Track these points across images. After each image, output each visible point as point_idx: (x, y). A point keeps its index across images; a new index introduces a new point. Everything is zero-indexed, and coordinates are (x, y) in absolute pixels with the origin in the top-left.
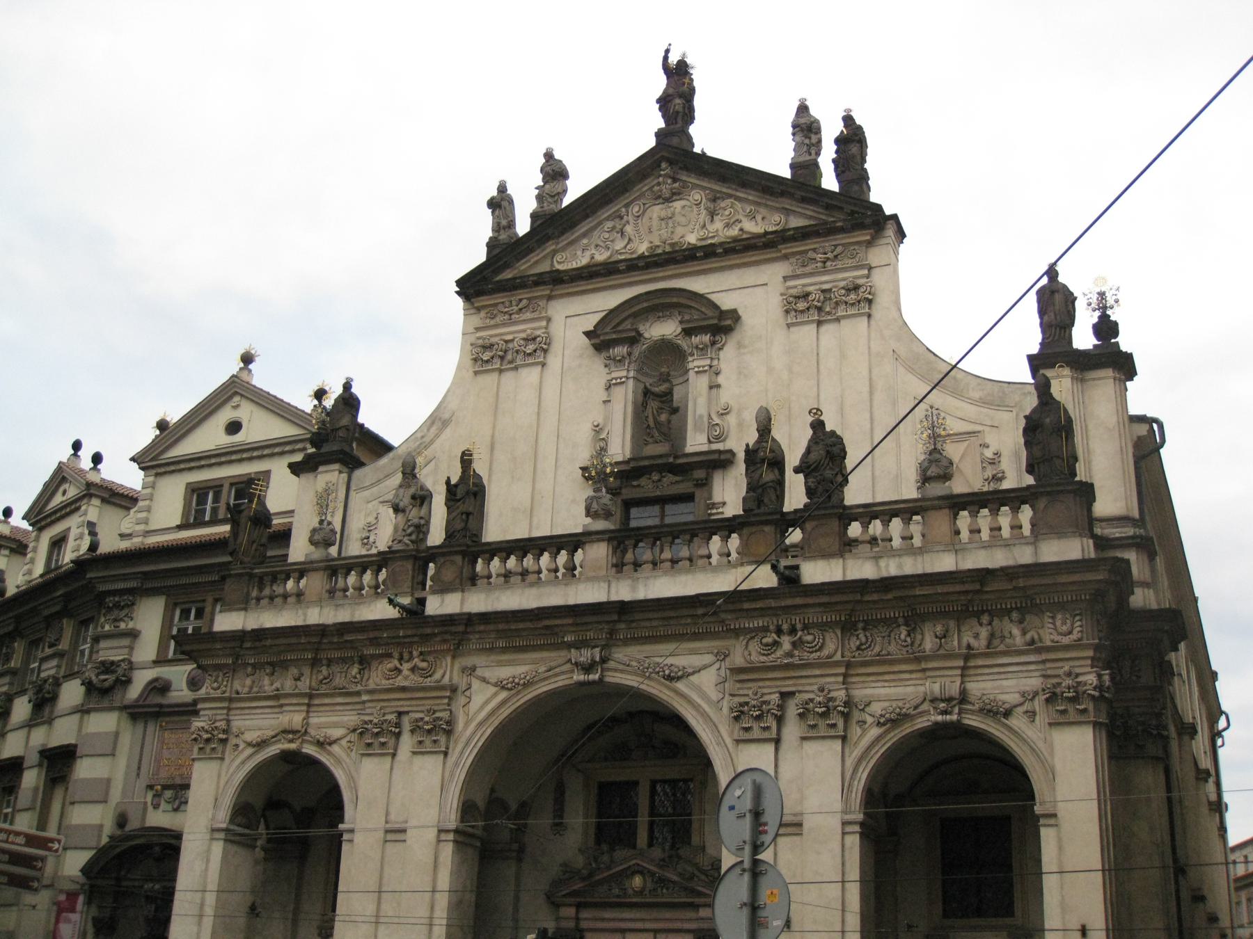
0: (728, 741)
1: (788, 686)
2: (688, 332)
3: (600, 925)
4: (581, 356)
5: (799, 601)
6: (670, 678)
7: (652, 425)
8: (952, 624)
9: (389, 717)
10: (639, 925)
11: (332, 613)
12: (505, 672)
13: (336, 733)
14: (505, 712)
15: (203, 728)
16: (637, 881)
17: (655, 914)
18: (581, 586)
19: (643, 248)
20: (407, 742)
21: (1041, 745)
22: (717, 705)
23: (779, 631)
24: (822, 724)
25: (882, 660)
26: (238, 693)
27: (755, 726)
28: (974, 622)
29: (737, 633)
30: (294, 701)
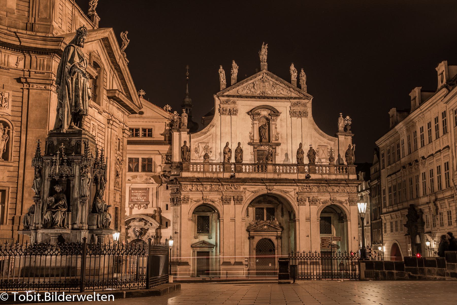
0: (297, 205)
1: (308, 196)
2: (271, 115)
3: (258, 235)
4: (245, 116)
5: (311, 182)
6: (285, 193)
7: (263, 134)
8: (335, 187)
9: (230, 197)
10: (266, 235)
11: (212, 174)
12: (253, 189)
13: (216, 199)
14: (254, 198)
15: (184, 198)
16: (266, 227)
17: (268, 232)
18: (268, 174)
19: (258, 92)
20: (232, 202)
21: (348, 209)
22: (294, 198)
23: (307, 186)
24: (314, 203)
25: (324, 192)
26: (191, 190)
27: (302, 202)
28: (338, 188)
29: (298, 186)
30: (206, 193)
